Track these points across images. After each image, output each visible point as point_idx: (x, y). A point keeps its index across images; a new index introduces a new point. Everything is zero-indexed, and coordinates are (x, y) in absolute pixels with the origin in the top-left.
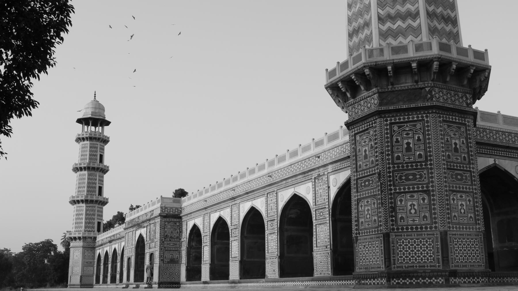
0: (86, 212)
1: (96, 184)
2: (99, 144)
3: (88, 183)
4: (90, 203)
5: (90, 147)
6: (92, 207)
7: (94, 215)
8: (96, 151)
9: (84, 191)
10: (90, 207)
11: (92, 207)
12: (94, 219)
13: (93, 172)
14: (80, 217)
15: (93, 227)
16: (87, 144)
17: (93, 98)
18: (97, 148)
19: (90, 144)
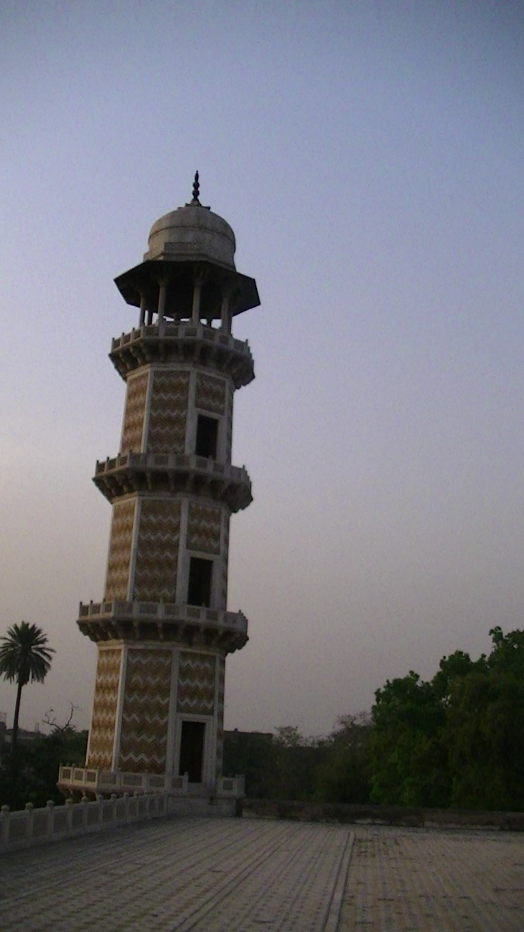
0: (127, 681)
1: (174, 547)
2: (194, 375)
3: (142, 545)
4: (142, 639)
5: (156, 389)
6: (157, 653)
7: (164, 691)
8: (182, 405)
9: (124, 583)
10: (144, 653)
11: (157, 653)
12: (163, 710)
13: (163, 496)
14: (109, 697)
15: (160, 749)
16: (144, 376)
17: (189, 199)
18: (184, 389)
19: (157, 374)
